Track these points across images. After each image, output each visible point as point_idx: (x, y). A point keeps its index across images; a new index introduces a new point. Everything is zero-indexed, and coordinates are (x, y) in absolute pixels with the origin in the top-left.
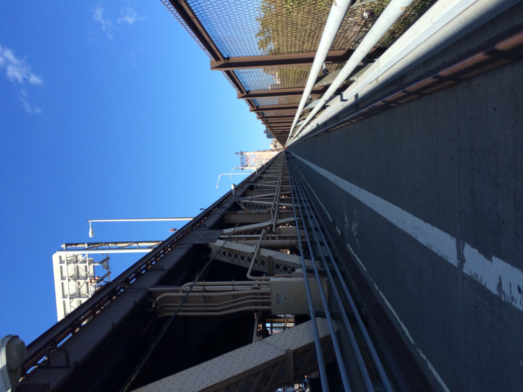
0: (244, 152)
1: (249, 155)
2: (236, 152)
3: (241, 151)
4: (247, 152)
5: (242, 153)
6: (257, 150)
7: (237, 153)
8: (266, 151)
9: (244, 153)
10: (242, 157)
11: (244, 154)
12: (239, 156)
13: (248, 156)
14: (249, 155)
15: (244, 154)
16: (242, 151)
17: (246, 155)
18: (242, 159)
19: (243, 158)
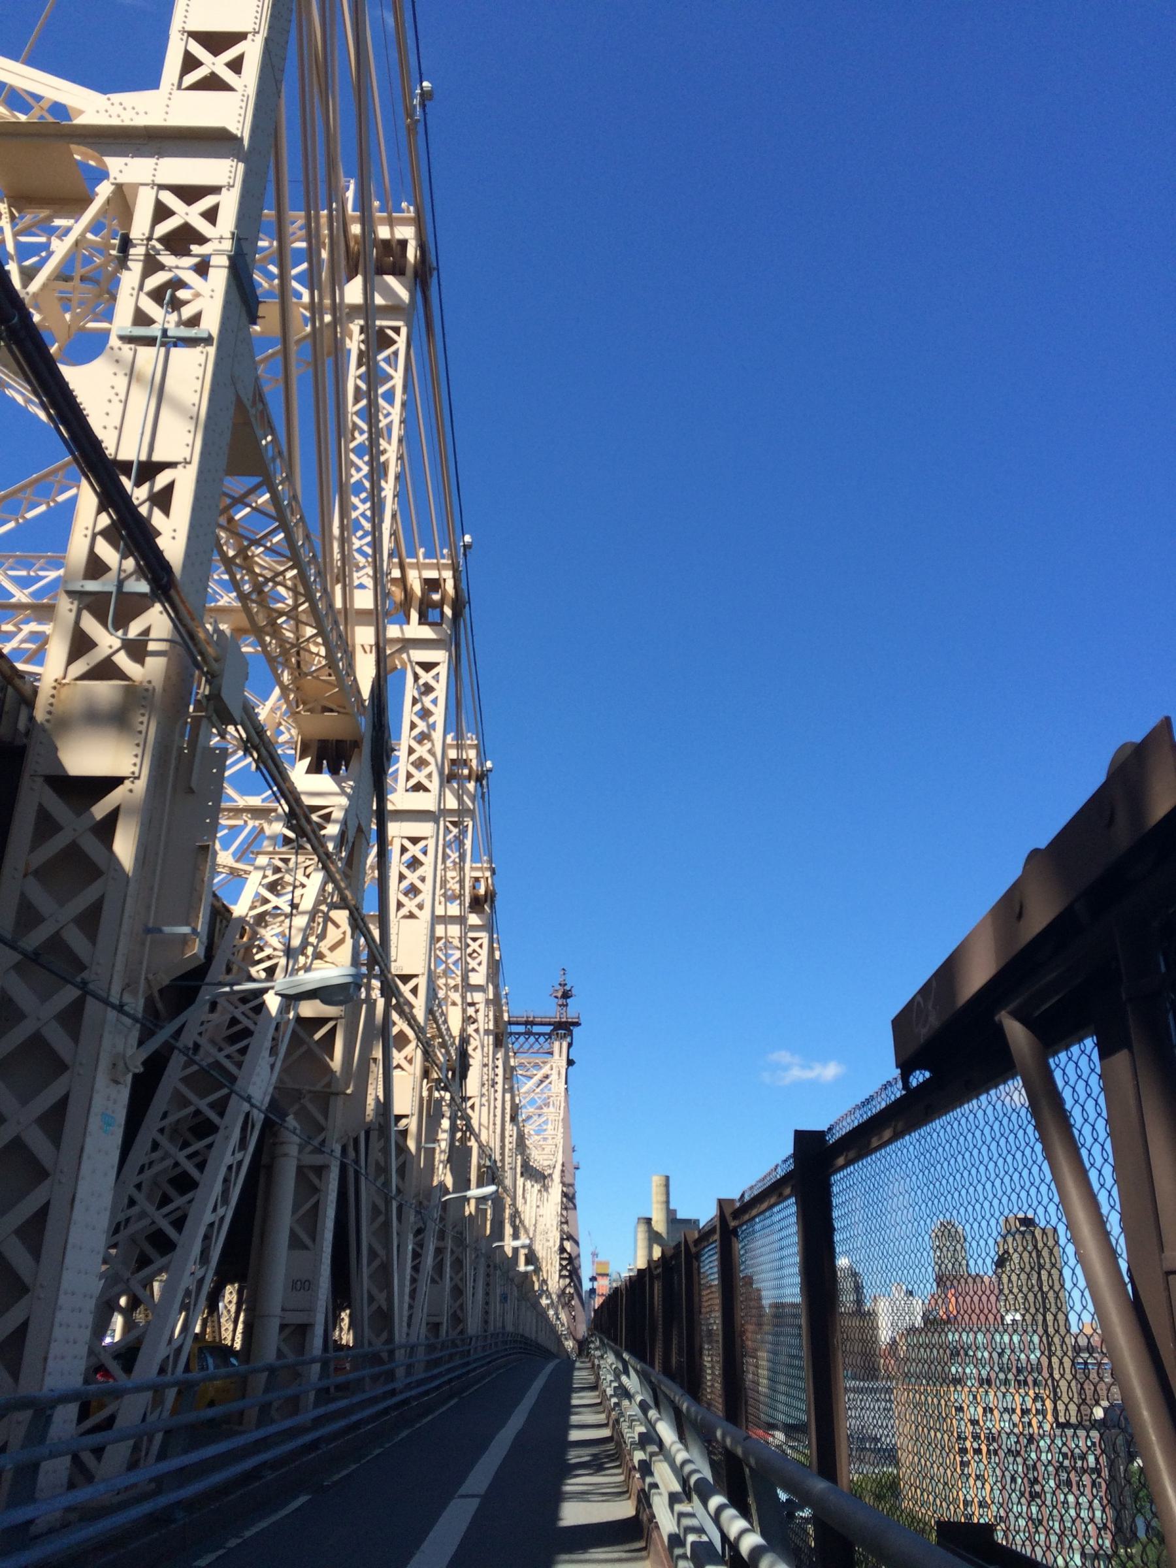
0: (570, 1045)
1: (550, 1083)
2: (574, 992)
3: (577, 1024)
4: (570, 1063)
5: (564, 1028)
6: (576, 1158)
7: (566, 995)
8: (565, 1208)
9: (565, 1045)
10: (536, 1029)
11: (559, 1048)
12: (550, 1010)
13: (548, 1066)
14: (550, 1083)
15: (557, 1044)
16: (576, 1030)
17: (551, 1053)
18: (521, 1029)
19: (529, 1034)
